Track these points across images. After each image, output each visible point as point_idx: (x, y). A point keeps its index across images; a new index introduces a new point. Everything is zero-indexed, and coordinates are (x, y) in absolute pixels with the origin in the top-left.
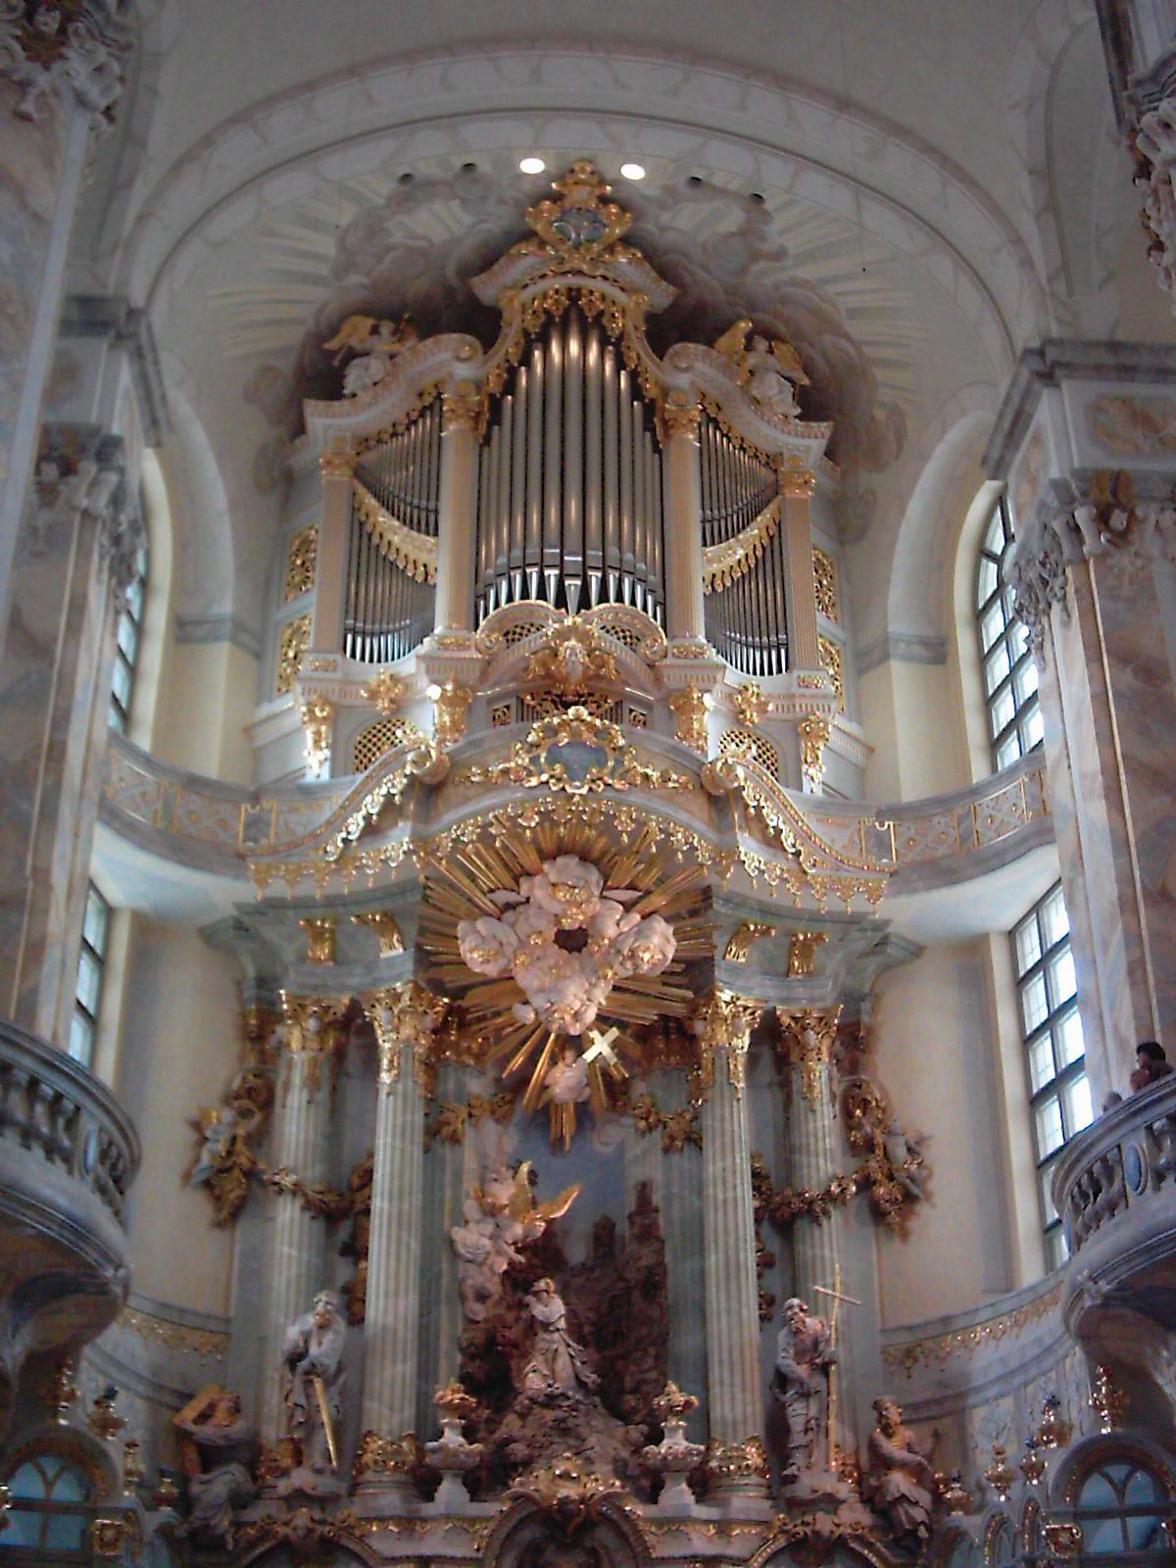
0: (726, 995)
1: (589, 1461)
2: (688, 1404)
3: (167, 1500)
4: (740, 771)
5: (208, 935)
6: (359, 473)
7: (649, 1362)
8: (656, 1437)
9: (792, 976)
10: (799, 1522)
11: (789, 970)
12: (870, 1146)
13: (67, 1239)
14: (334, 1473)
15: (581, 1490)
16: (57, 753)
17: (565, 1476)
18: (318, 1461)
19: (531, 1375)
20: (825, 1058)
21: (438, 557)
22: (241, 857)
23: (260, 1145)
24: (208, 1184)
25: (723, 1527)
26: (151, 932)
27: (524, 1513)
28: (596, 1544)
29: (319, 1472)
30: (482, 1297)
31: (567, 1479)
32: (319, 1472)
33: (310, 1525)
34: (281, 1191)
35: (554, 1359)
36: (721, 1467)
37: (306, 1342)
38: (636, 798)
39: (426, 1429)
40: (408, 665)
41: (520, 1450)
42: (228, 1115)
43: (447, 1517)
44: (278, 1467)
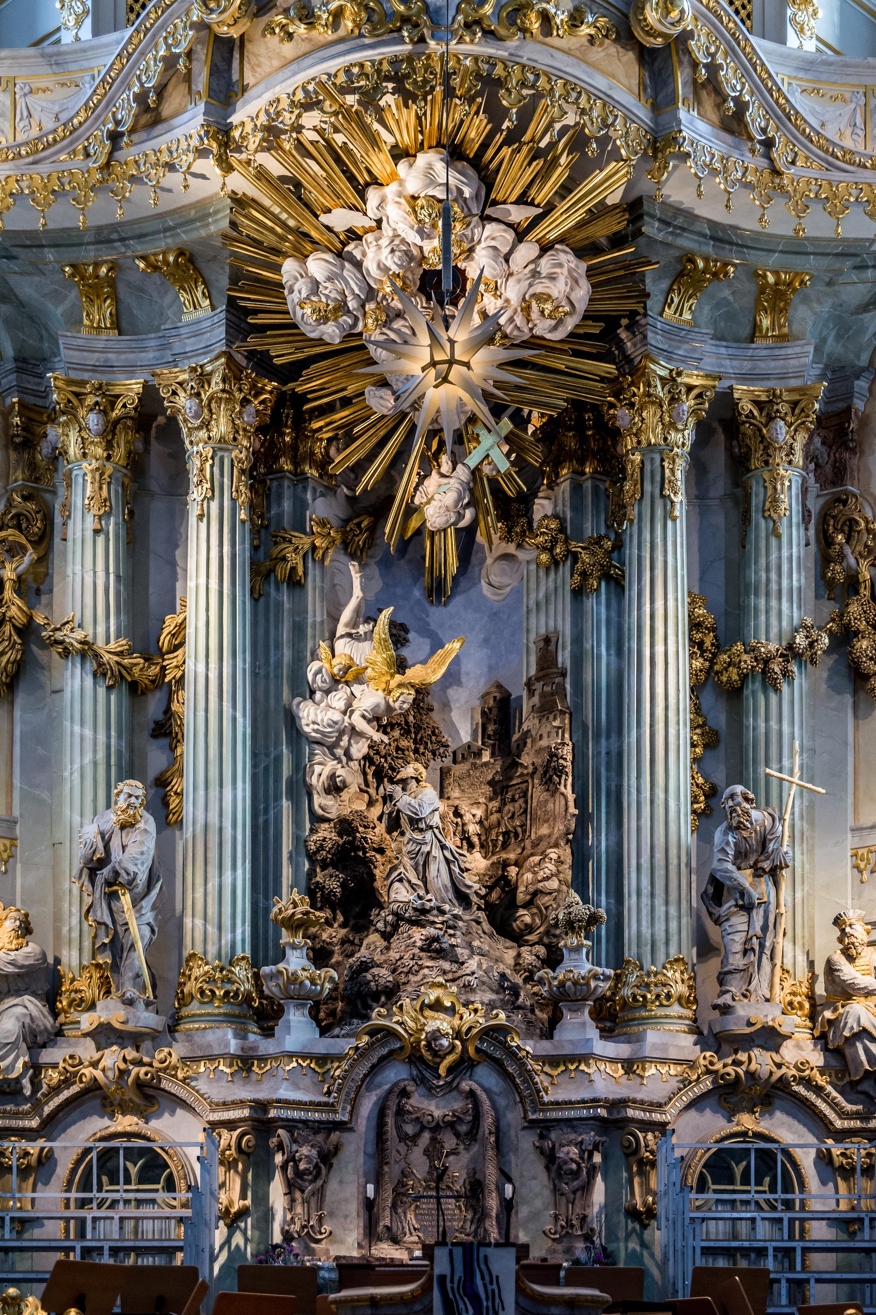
1: (468, 988)
2: (593, 919)
7: (550, 867)
8: (553, 959)
9: (759, 343)
10: (729, 1060)
14: (148, 1004)
15: (456, 1022)
17: (437, 1006)
18: (131, 992)
19: (397, 885)
20: (798, 458)
23: (38, 592)
27: (385, 1051)
28: (475, 1086)
29: (130, 1003)
32: (130, 1003)
33: (123, 1066)
34: (66, 653)
35: (426, 864)
36: (634, 996)
37: (107, 847)
43: (291, 1055)
44: (82, 1000)
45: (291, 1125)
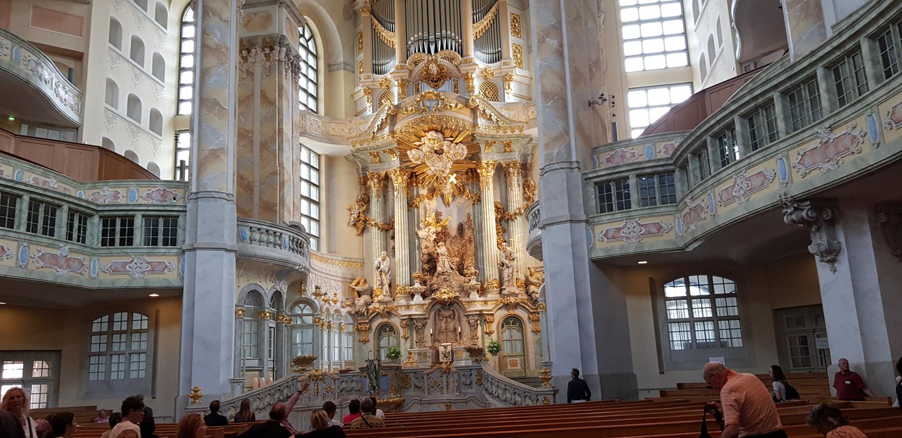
0: (484, 161)
3: (348, 306)
4: (477, 100)
5: (346, 158)
6: (372, 13)
11: (505, 151)
12: (529, 198)
13: (282, 264)
16: (281, 131)
21: (394, 38)
22: (348, 138)
24: (354, 225)
25: (486, 302)
26: (331, 160)
30: (427, 247)
31: (444, 294)
38: (448, 113)
39: (412, 284)
40: (388, 76)
41: (436, 286)
42: (357, 207)
45: (416, 319)
